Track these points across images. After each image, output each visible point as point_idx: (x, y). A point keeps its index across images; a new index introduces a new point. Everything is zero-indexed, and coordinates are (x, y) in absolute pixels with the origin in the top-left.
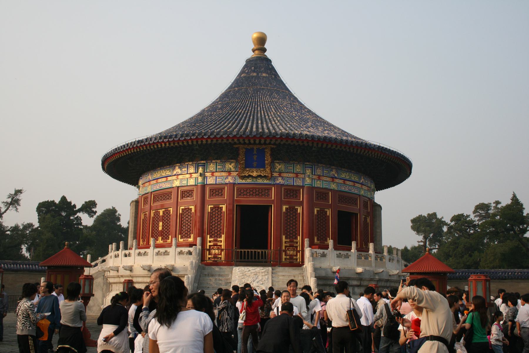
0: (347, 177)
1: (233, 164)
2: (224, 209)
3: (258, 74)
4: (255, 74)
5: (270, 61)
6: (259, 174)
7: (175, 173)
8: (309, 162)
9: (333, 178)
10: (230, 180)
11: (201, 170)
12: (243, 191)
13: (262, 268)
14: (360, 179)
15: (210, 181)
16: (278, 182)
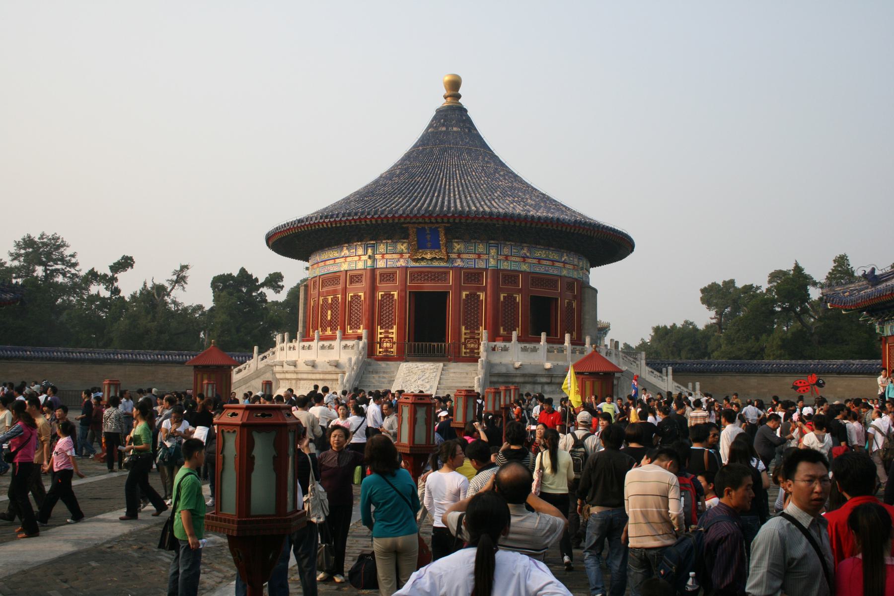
0: (543, 256)
1: (405, 245)
2: (396, 297)
3: (447, 129)
4: (444, 129)
5: (466, 111)
6: (434, 256)
7: (343, 254)
8: (493, 239)
9: (524, 258)
10: (402, 263)
11: (370, 251)
12: (417, 275)
13: (432, 364)
14: (562, 256)
15: (381, 264)
16: (456, 265)
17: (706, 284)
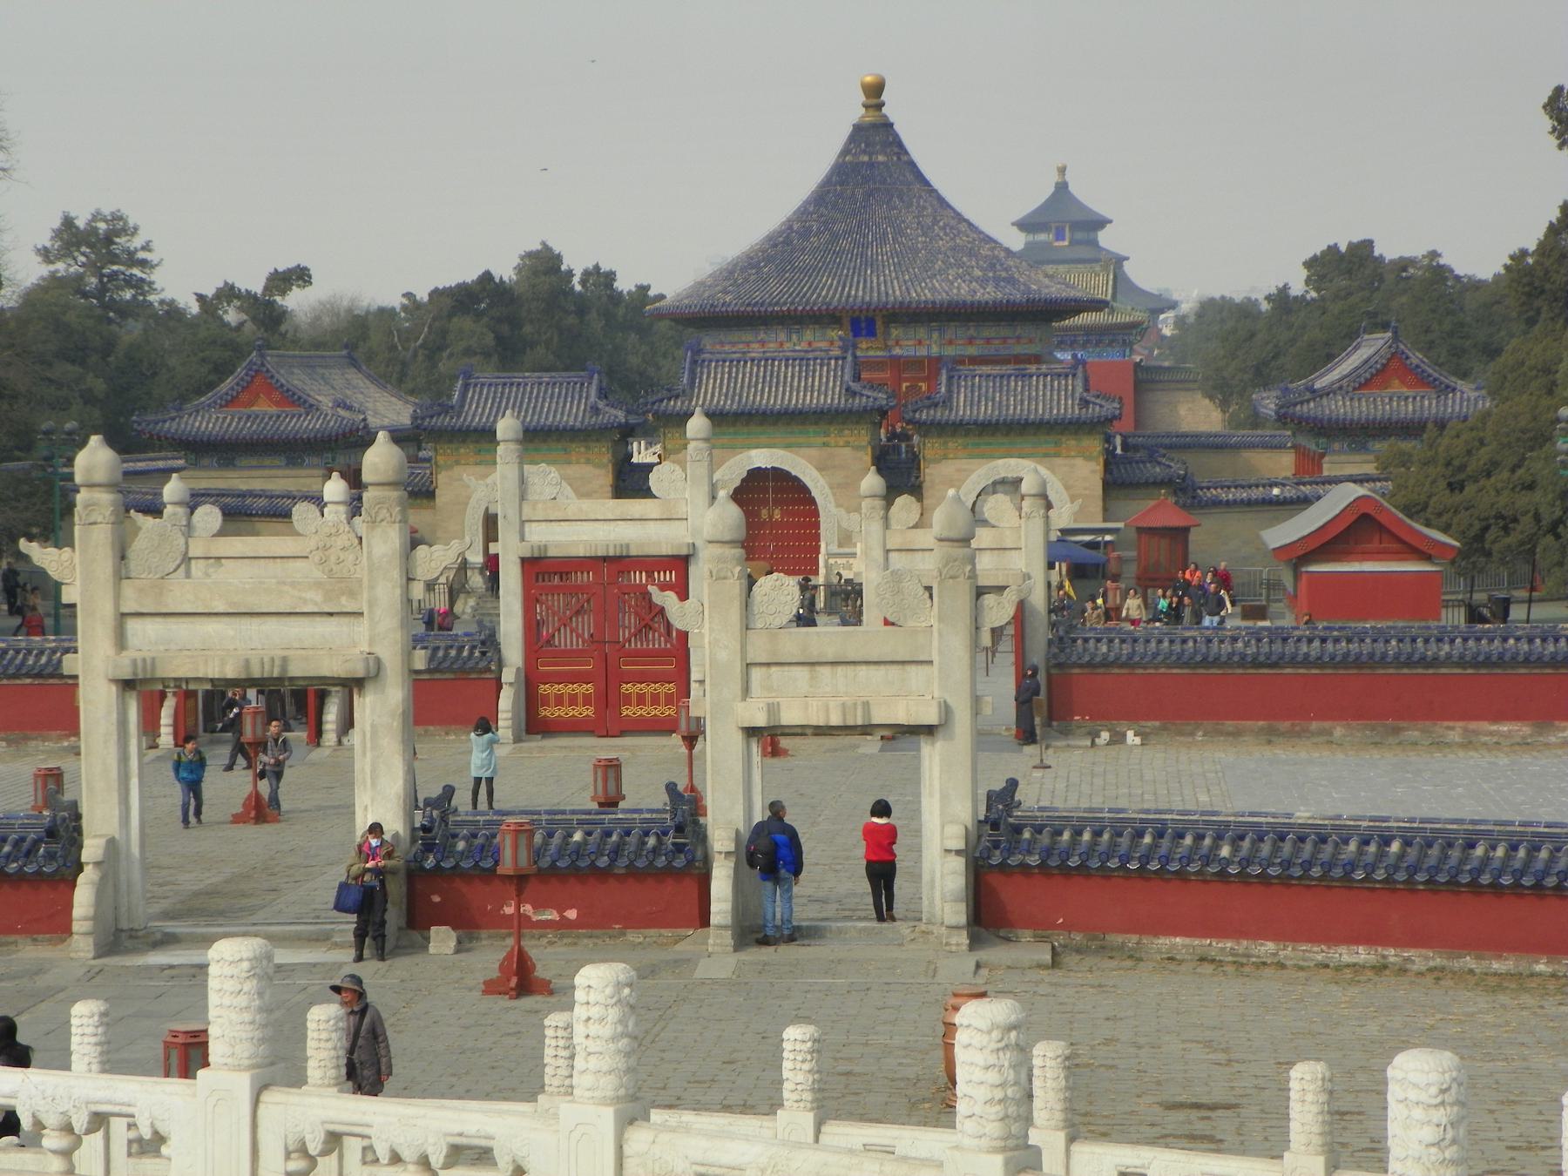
11: (794, 337)
17: (1318, 248)
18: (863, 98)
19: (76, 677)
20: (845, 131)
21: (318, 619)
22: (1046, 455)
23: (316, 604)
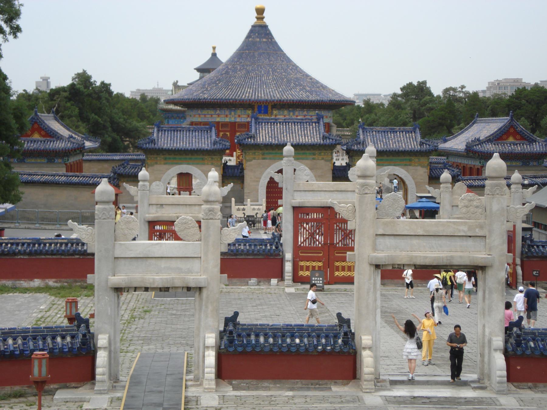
4: (258, 40)
11: (233, 113)
15: (238, 120)
18: (256, 15)
19: (93, 255)
20: (249, 28)
21: (465, 238)
22: (406, 165)
23: (464, 231)
